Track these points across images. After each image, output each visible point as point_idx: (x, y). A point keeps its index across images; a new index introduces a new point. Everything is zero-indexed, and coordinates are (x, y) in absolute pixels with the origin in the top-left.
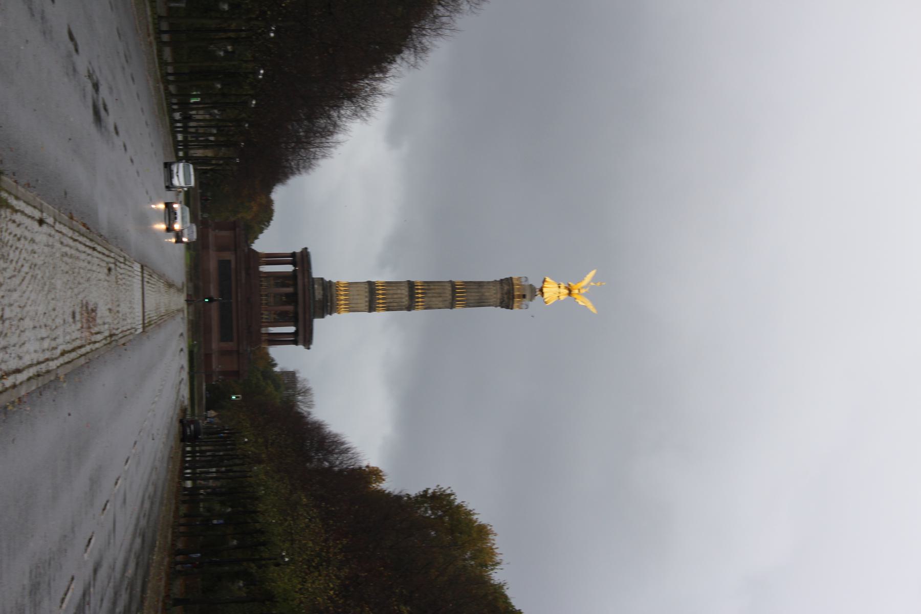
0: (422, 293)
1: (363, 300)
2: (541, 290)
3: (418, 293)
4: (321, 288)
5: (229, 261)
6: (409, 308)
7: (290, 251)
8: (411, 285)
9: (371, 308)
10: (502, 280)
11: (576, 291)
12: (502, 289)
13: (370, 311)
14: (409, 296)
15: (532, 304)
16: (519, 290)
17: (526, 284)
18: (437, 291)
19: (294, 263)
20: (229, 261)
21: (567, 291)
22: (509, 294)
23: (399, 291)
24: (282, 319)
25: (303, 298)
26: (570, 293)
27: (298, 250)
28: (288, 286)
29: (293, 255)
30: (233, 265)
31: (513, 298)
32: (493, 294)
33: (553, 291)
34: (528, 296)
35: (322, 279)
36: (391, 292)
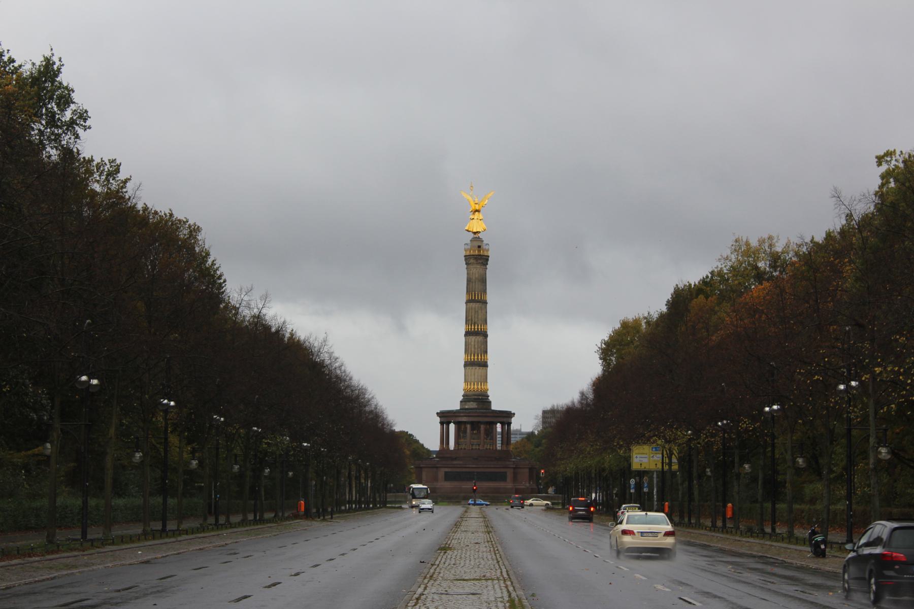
1: (478, 370)
2: (475, 233)
5: (446, 473)
6: (485, 335)
9: (485, 365)
12: (473, 264)
13: (486, 366)
16: (474, 251)
19: (448, 423)
20: (446, 473)
24: (490, 433)
25: (476, 416)
26: (478, 211)
27: (438, 419)
28: (466, 428)
29: (442, 423)
32: (476, 270)
33: (477, 225)
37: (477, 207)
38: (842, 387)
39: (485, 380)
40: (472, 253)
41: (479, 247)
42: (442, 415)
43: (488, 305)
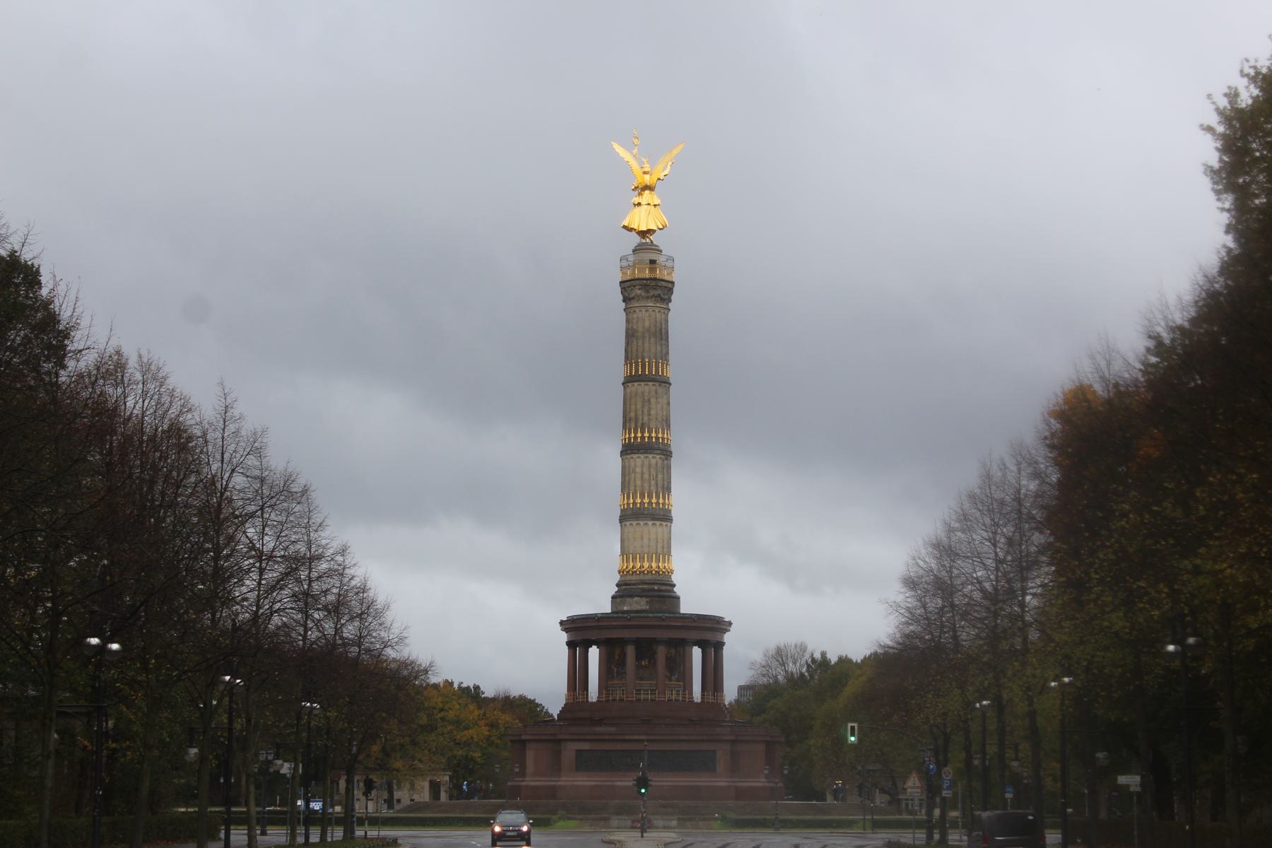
0: (643, 432)
1: (651, 530)
2: (643, 234)
3: (643, 438)
4: (628, 600)
5: (578, 751)
6: (666, 453)
8: (628, 449)
9: (664, 517)
11: (647, 177)
12: (638, 298)
14: (645, 447)
17: (631, 258)
19: (587, 644)
21: (647, 192)
22: (647, 287)
23: (638, 470)
24: (679, 668)
25: (643, 635)
26: (650, 188)
27: (564, 637)
28: (623, 655)
29: (571, 645)
31: (655, 279)
32: (647, 314)
33: (642, 219)
34: (653, 257)
35: (613, 597)
36: (639, 483)
37: (647, 179)
38: (1191, 640)
39: (665, 551)
40: (637, 275)
41: (653, 262)
42: (571, 625)
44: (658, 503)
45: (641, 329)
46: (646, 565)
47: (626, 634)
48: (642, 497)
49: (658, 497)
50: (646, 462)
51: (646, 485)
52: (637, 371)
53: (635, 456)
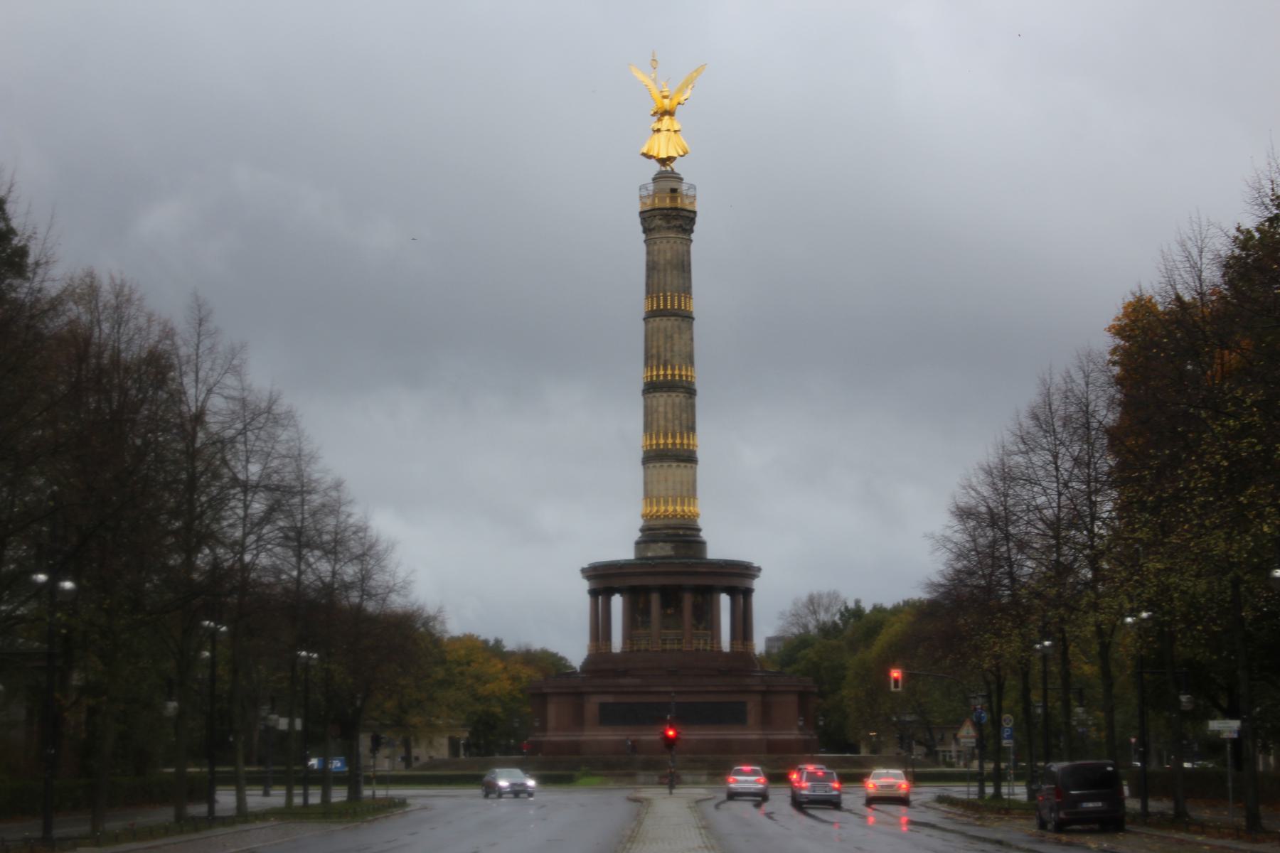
0: (665, 369)
1: (675, 472)
2: (663, 162)
4: (653, 546)
5: (603, 706)
6: (690, 391)
7: (586, 600)
8: (651, 388)
9: (688, 458)
10: (646, 230)
11: (666, 101)
12: (659, 229)
15: (688, 178)
17: (651, 187)
18: (661, 343)
20: (603, 706)
21: (666, 118)
22: (669, 217)
23: (661, 409)
25: (671, 580)
26: (669, 113)
27: (585, 585)
29: (594, 593)
30: (609, 699)
31: (676, 209)
32: (668, 245)
34: (674, 185)
35: (638, 543)
36: (662, 423)
40: (658, 204)
41: (674, 191)
43: (696, 324)
44: (682, 444)
45: (662, 262)
46: (671, 509)
47: (650, 581)
48: (666, 436)
49: (682, 438)
50: (670, 401)
51: (670, 425)
52: (658, 305)
53: (657, 395)
